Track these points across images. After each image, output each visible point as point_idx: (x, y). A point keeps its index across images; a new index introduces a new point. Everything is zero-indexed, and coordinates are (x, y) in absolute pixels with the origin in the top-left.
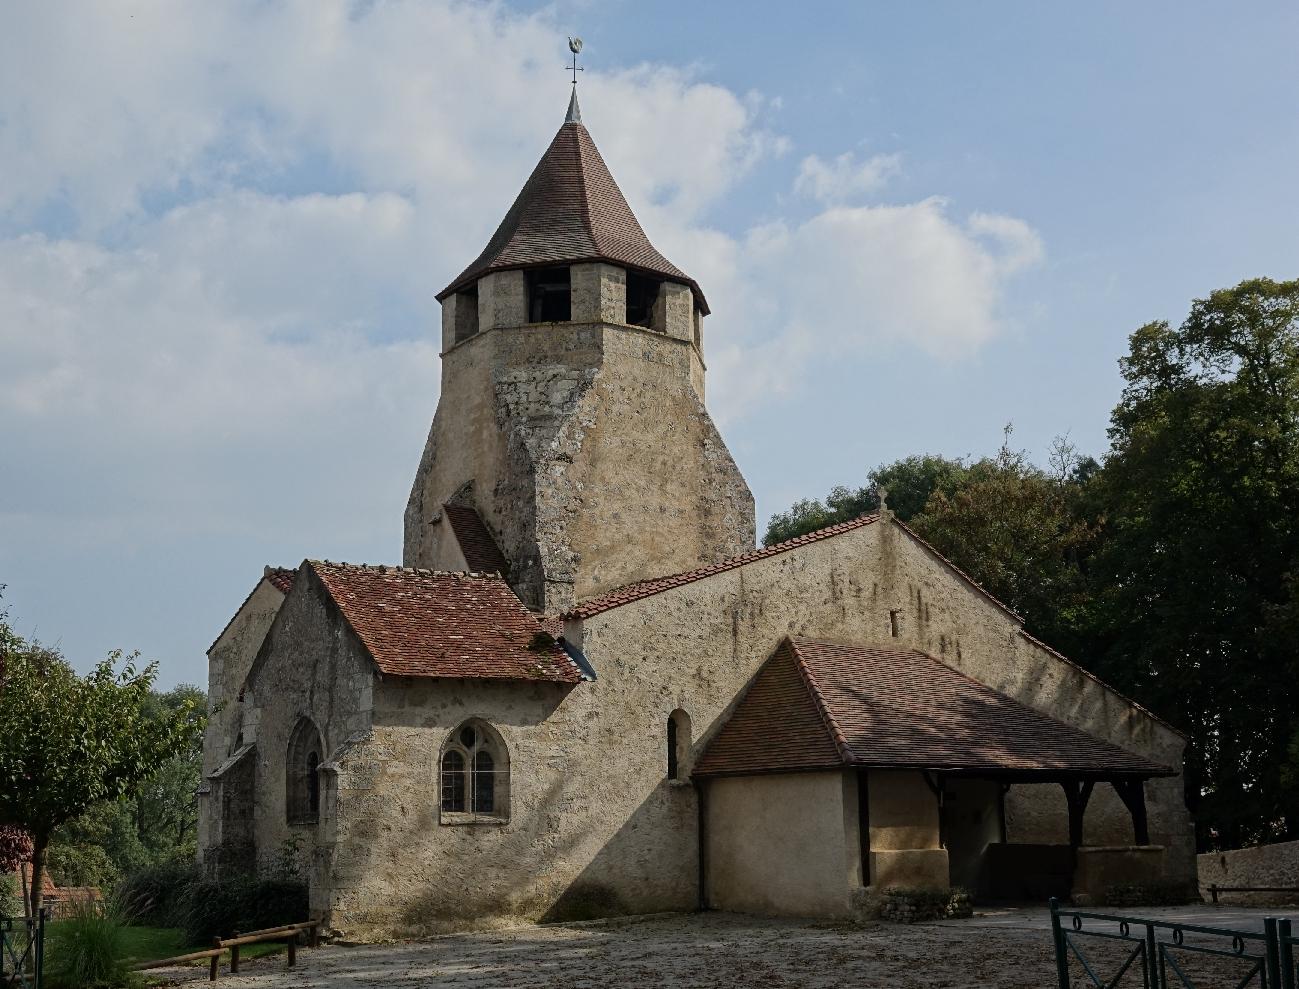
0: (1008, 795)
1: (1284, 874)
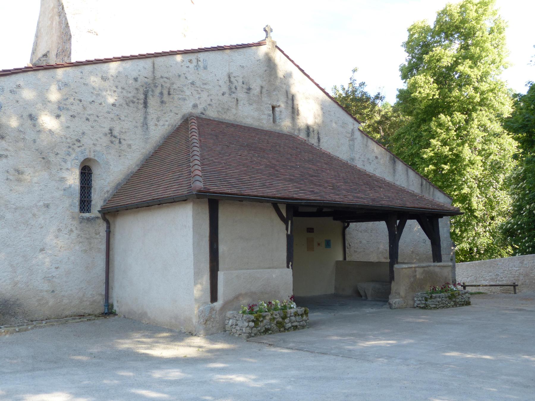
0: (347, 229)
1: (497, 275)
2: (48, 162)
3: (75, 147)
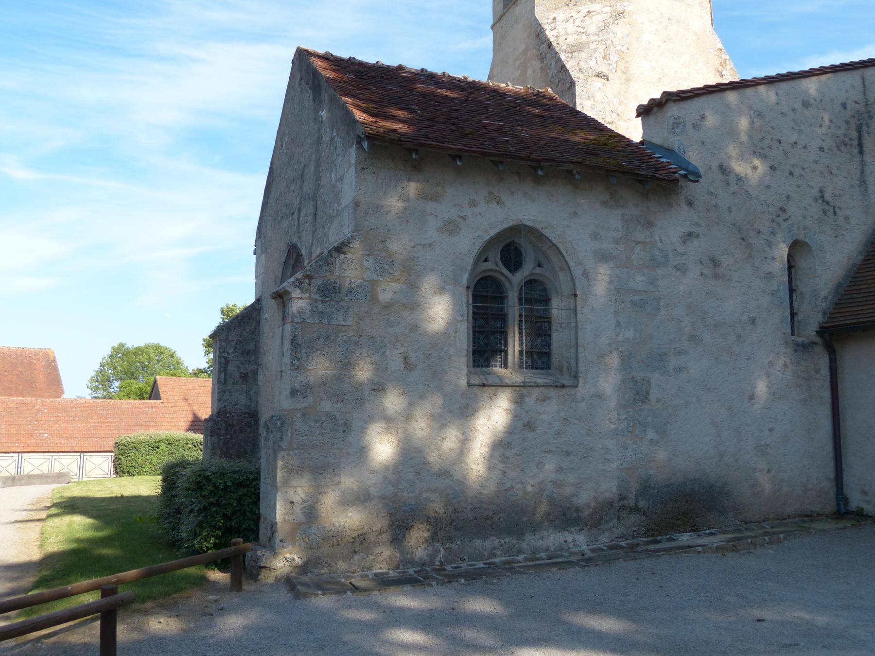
2: (749, 246)
3: (780, 220)
